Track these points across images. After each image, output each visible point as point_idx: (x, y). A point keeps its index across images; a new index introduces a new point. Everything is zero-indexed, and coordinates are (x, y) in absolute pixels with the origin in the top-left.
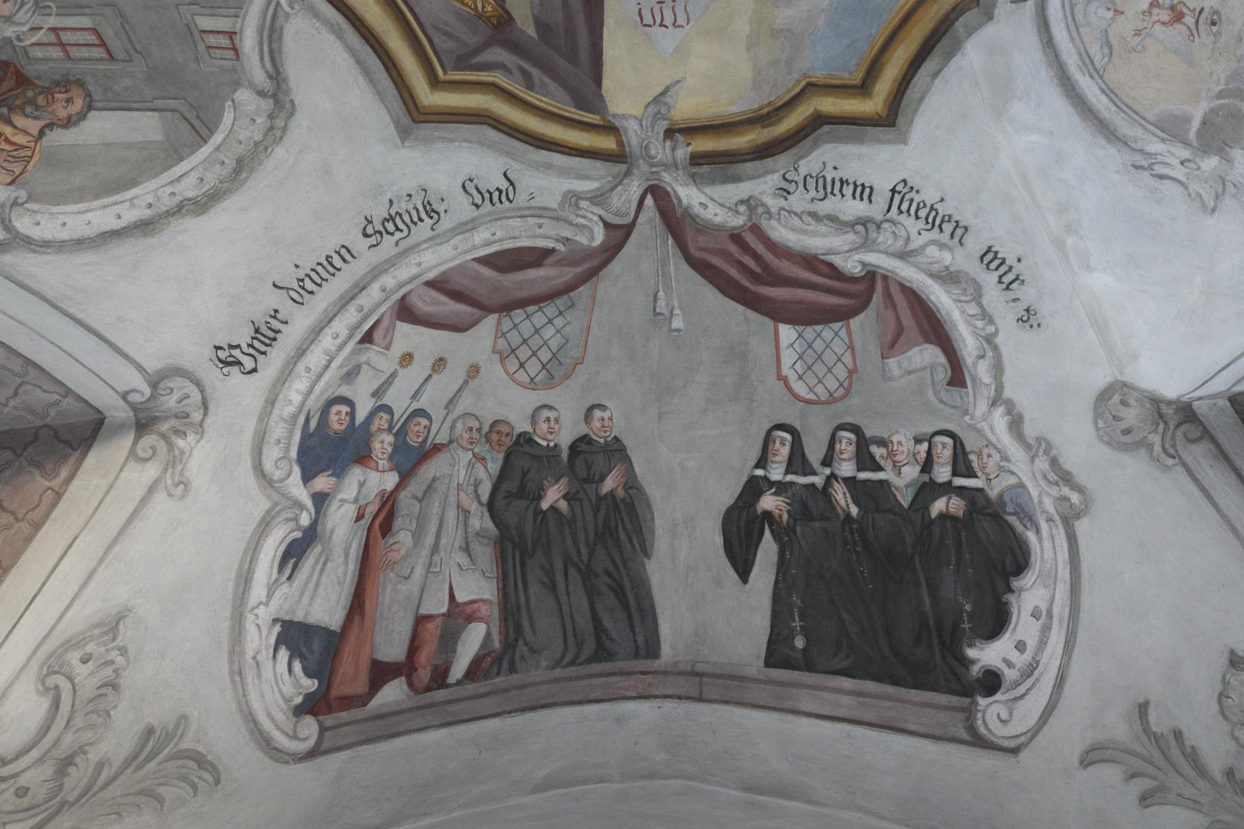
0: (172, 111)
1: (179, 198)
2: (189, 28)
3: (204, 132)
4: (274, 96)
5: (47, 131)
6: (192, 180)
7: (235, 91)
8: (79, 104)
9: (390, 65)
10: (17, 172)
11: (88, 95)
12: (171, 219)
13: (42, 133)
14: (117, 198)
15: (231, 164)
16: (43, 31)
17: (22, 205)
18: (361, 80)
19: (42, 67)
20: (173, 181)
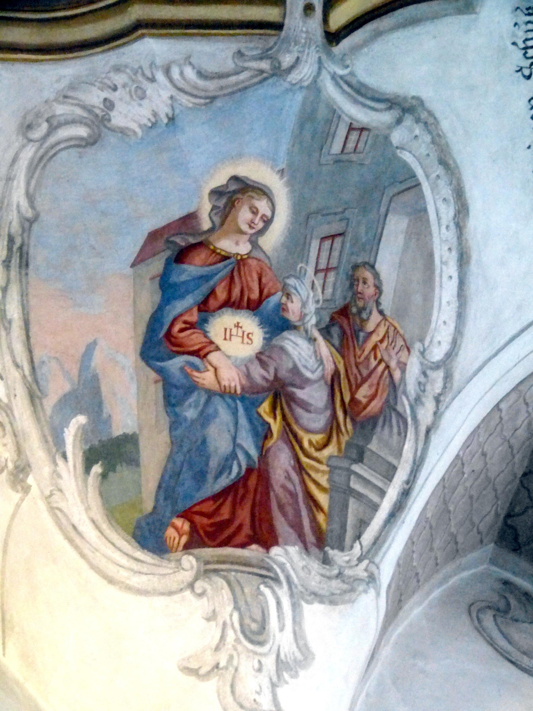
0: (390, 201)
1: (452, 225)
5: (381, 308)
6: (443, 208)
7: (391, 143)
8: (368, 275)
10: (402, 343)
11: (365, 264)
13: (381, 312)
14: (437, 272)
15: (440, 170)
16: (316, 282)
18: (417, 29)
19: (339, 293)
20: (439, 223)
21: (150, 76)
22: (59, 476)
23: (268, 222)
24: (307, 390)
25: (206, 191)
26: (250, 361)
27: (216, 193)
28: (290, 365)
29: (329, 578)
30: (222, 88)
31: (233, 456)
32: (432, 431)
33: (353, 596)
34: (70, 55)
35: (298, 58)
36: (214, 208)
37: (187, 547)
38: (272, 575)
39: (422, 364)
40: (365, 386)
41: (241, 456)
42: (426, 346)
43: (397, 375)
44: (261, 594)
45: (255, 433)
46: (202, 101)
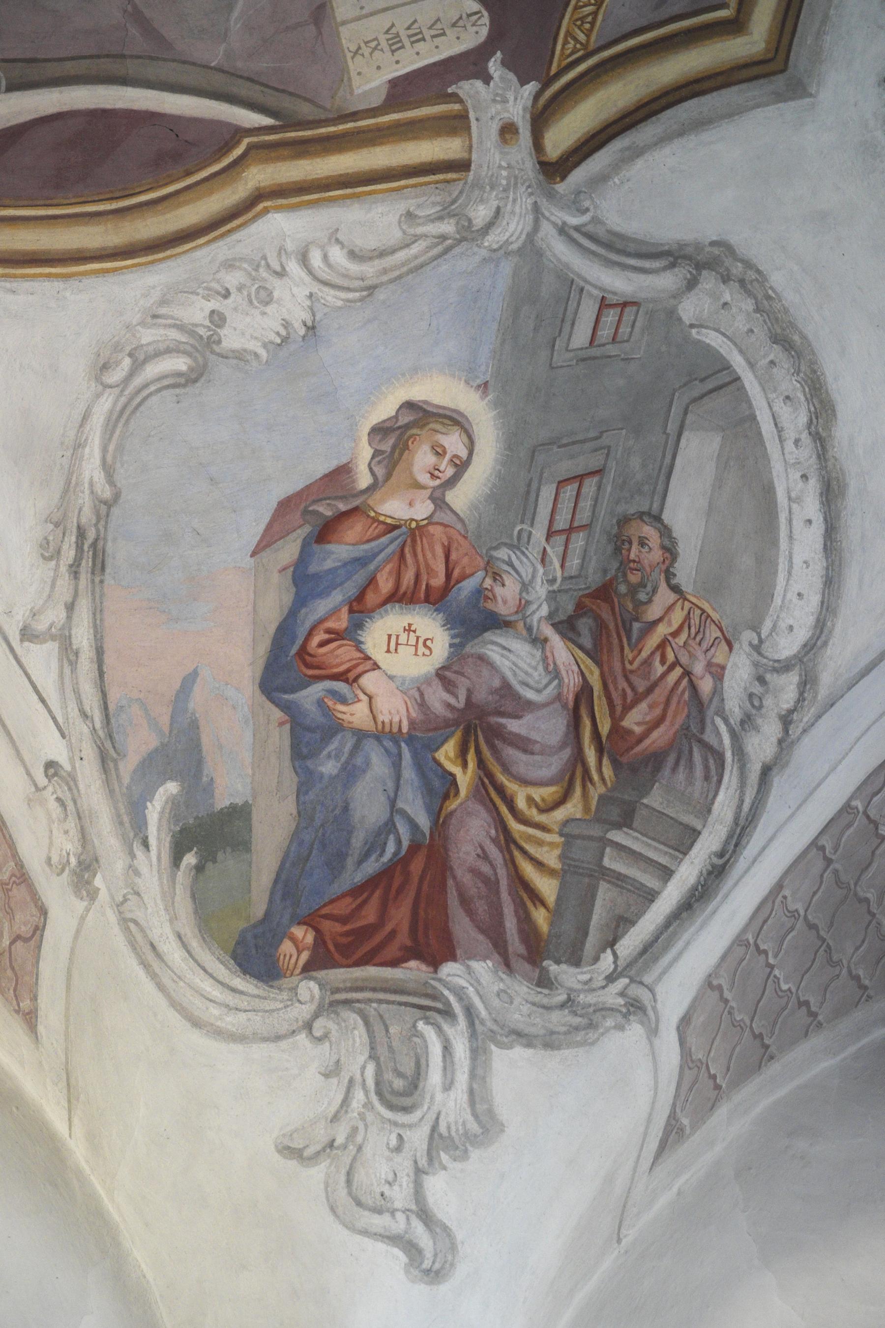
0: (686, 412)
1: (805, 437)
2: (584, 360)
3: (724, 377)
4: (700, 266)
5: (674, 582)
6: (784, 412)
7: (680, 319)
8: (649, 531)
9: (697, 87)
10: (719, 634)
12: (830, 454)
15: (776, 353)
16: (548, 549)
17: (761, 641)
18: (706, 136)
19: (593, 566)
20: (780, 437)
21: (278, 268)
22: (137, 873)
23: (461, 466)
24: (528, 718)
25: (366, 429)
26: (427, 681)
27: (379, 431)
28: (497, 683)
29: (547, 1008)
30: (385, 271)
31: (389, 826)
32: (775, 771)
33: (592, 1035)
34: (161, 255)
35: (498, 210)
36: (377, 453)
37: (308, 968)
38: (439, 1005)
39: (756, 665)
40: (643, 706)
41: (403, 829)
42: (764, 634)
43: (706, 685)
44: (421, 1036)
45: (428, 789)
46: (357, 294)
